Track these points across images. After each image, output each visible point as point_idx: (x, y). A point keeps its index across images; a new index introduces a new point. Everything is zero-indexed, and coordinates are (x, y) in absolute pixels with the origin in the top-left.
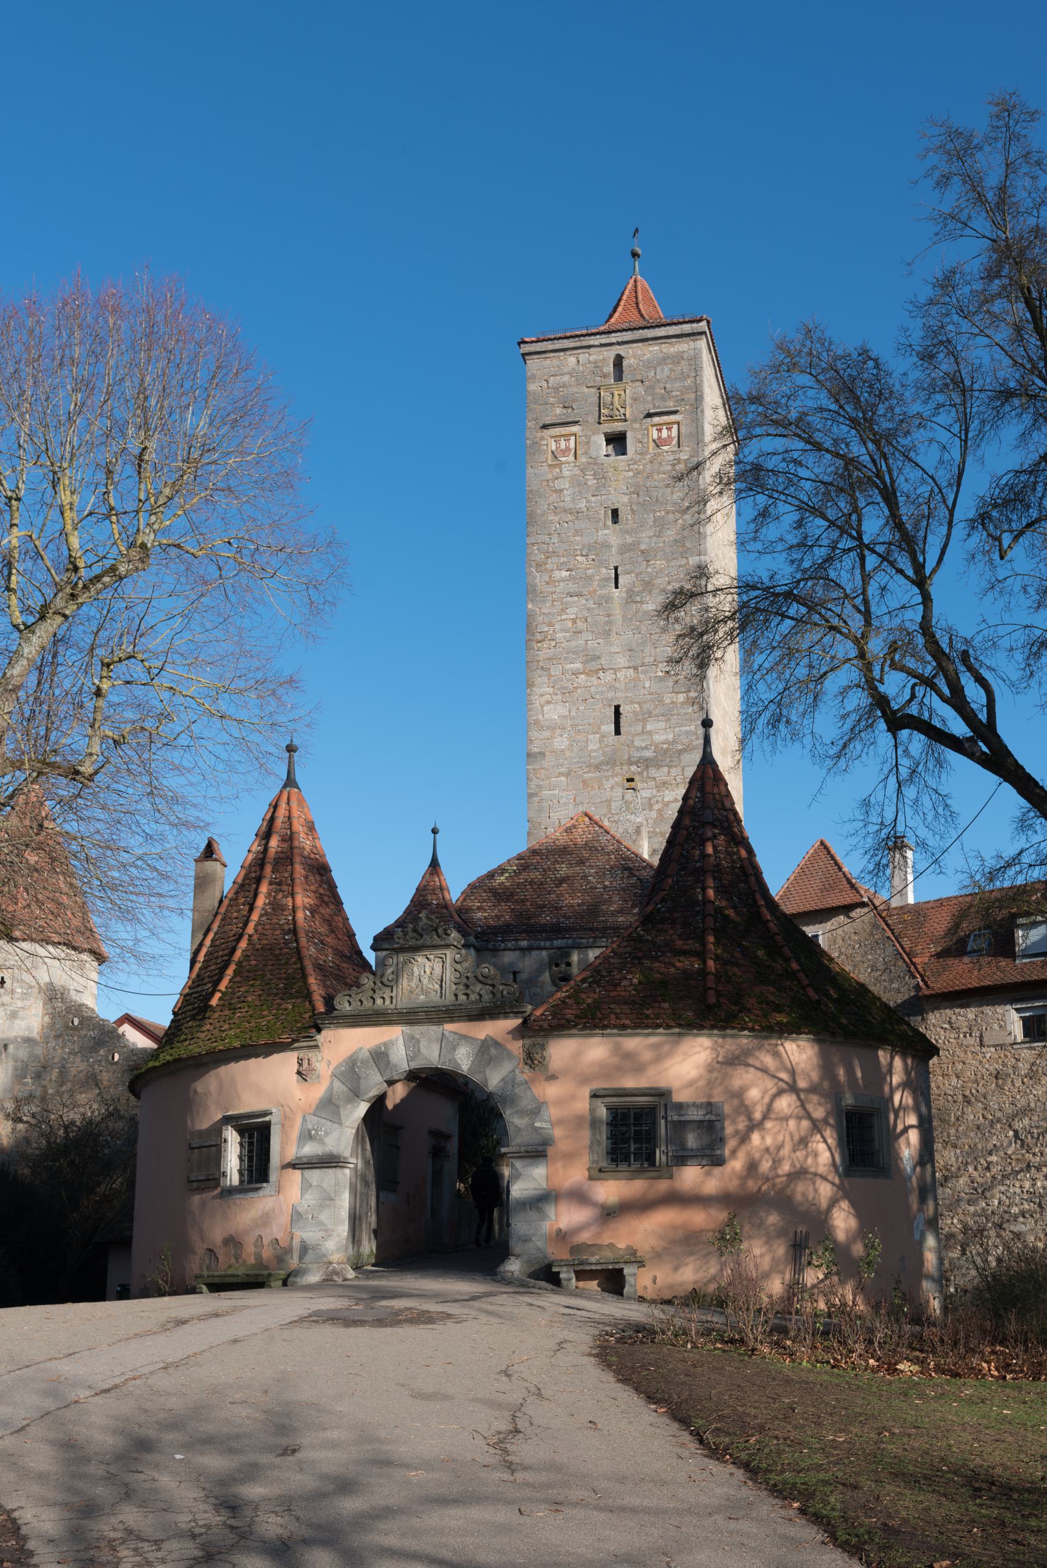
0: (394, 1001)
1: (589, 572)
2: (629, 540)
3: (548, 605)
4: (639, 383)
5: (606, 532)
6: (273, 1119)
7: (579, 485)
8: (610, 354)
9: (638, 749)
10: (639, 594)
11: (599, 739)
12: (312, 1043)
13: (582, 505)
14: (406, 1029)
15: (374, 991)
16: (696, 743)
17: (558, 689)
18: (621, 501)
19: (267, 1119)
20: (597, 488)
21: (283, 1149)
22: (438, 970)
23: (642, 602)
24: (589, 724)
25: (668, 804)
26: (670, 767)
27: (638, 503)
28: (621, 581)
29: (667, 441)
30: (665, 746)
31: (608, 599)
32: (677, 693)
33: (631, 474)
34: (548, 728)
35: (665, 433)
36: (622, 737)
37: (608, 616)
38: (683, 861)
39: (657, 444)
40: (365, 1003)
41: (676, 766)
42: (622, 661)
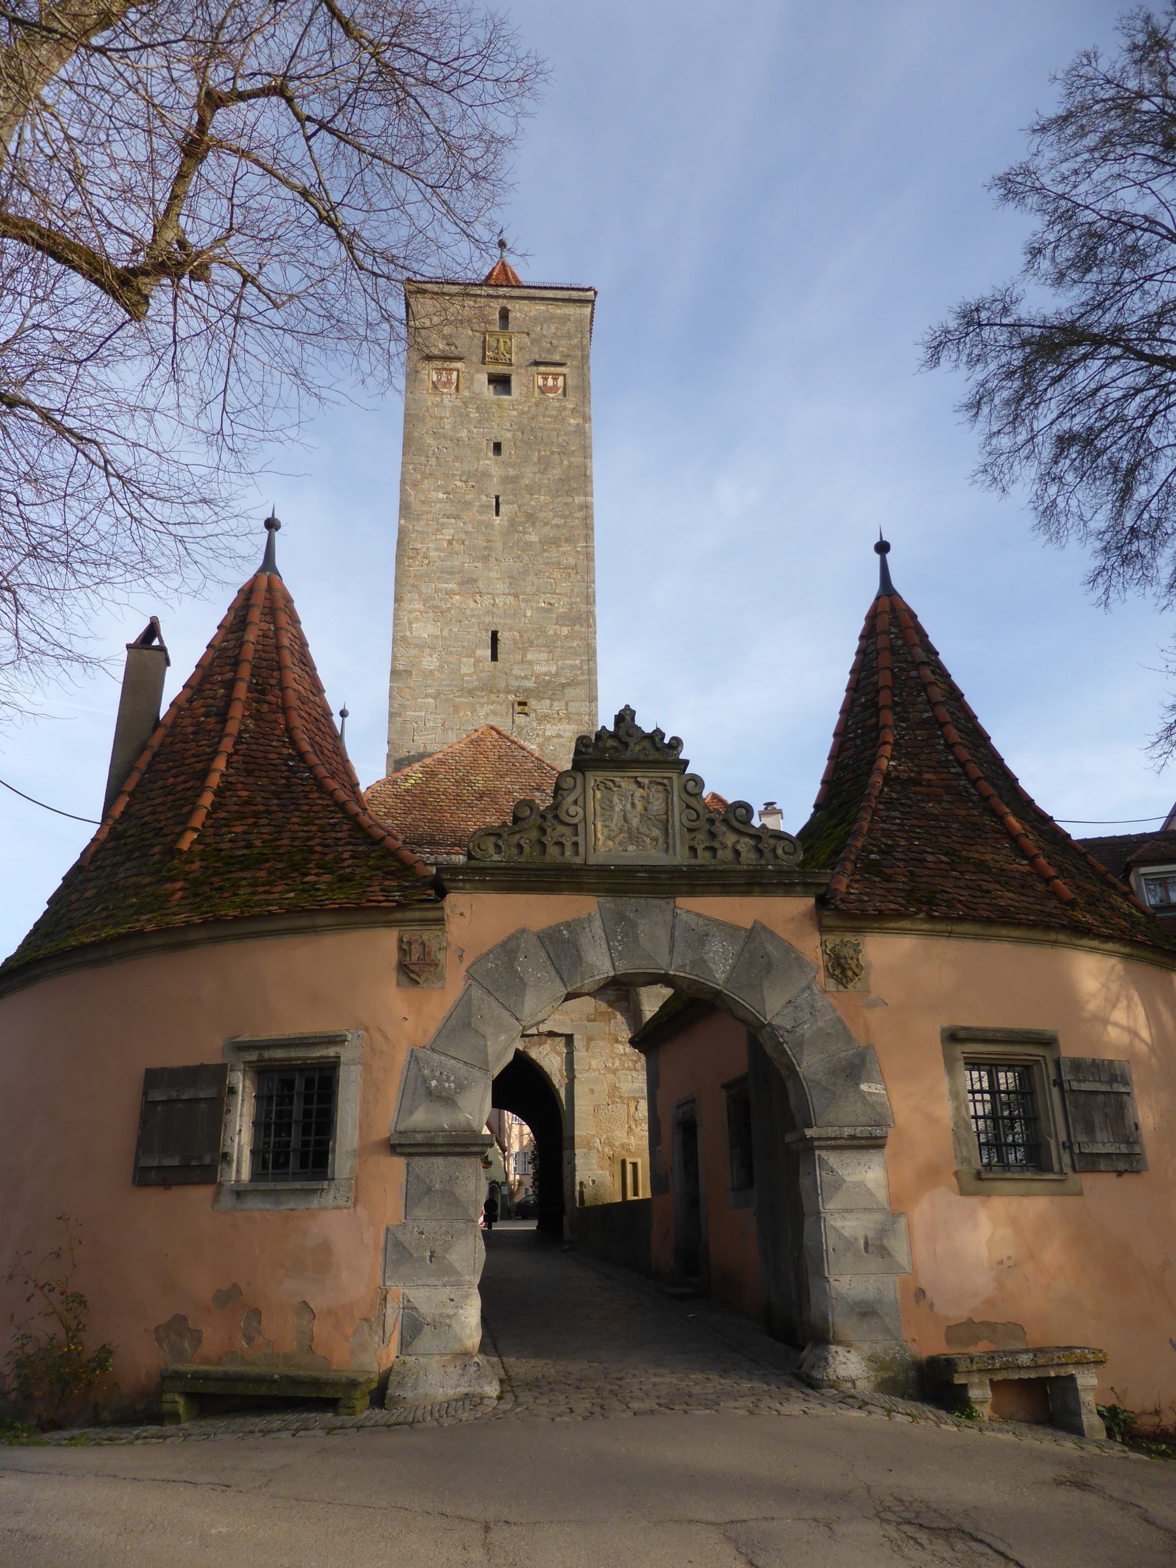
0: (581, 850)
1: (469, 497)
2: (512, 472)
3: (422, 523)
4: (524, 335)
5: (488, 462)
6: (346, 1053)
7: (461, 415)
8: (496, 305)
9: (517, 678)
10: (521, 524)
11: (474, 662)
12: (431, 915)
13: (464, 434)
14: (608, 902)
15: (543, 831)
16: (581, 678)
17: (430, 607)
18: (506, 437)
19: (331, 1052)
20: (480, 421)
21: (365, 1112)
22: (657, 805)
23: (525, 533)
24: (463, 647)
25: (549, 738)
26: (552, 700)
27: (522, 441)
28: (502, 509)
29: (554, 389)
30: (547, 678)
31: (489, 525)
32: (561, 626)
33: (515, 413)
34: (416, 646)
35: (550, 382)
36: (499, 664)
37: (488, 541)
38: (898, 709)
39: (544, 390)
40: (527, 849)
41: (559, 700)
42: (501, 587)
